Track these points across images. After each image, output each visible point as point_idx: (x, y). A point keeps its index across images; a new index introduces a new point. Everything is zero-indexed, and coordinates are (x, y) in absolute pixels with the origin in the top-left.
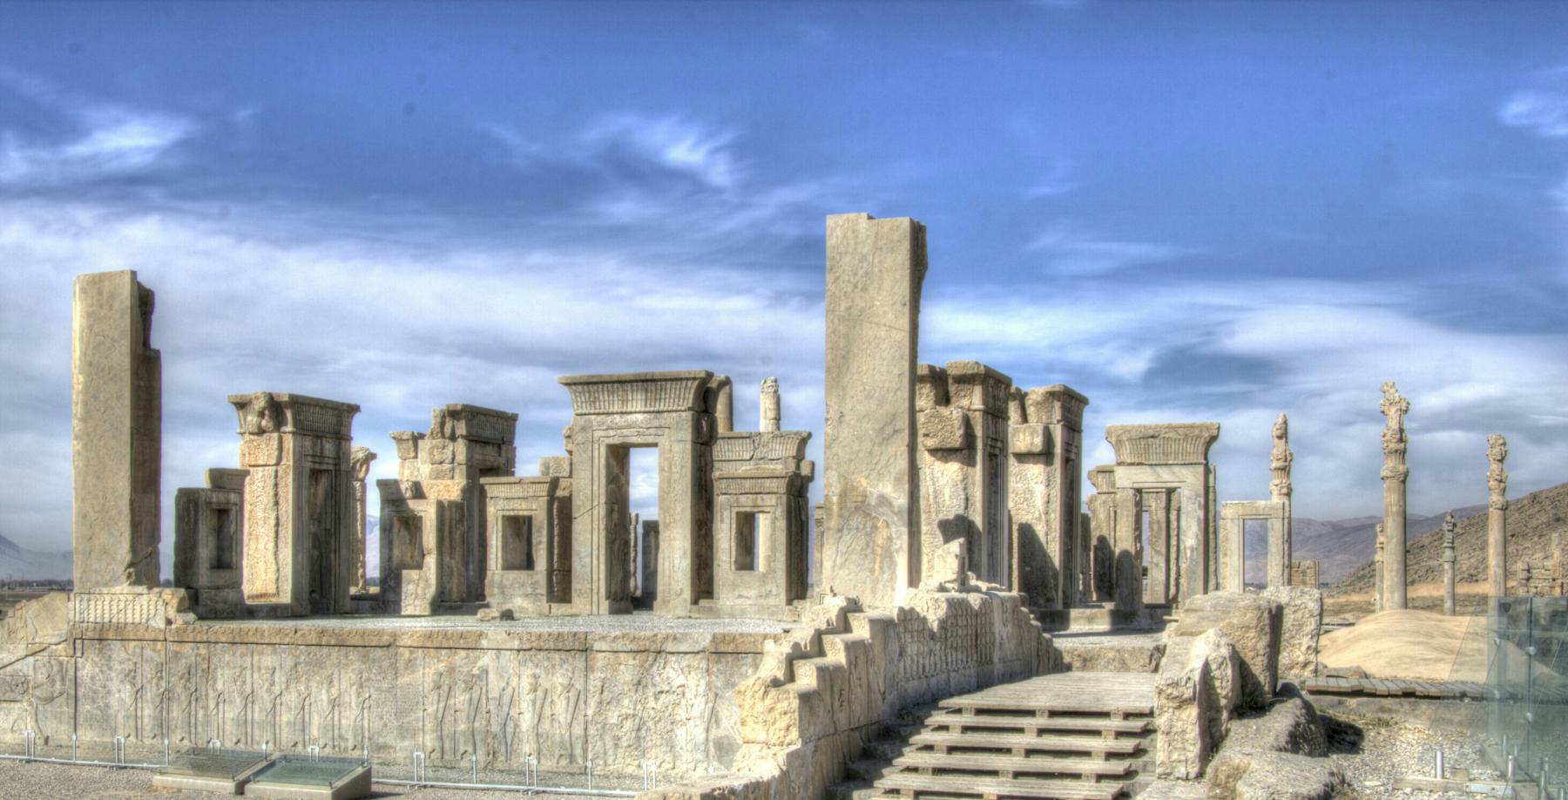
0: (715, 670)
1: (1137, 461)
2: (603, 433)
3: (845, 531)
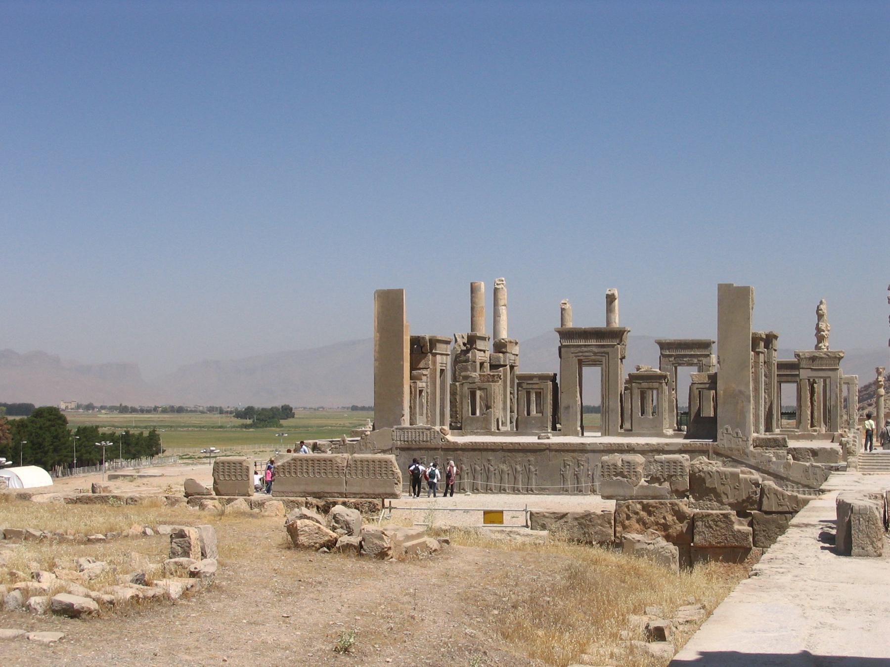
1: (808, 367)
2: (576, 355)
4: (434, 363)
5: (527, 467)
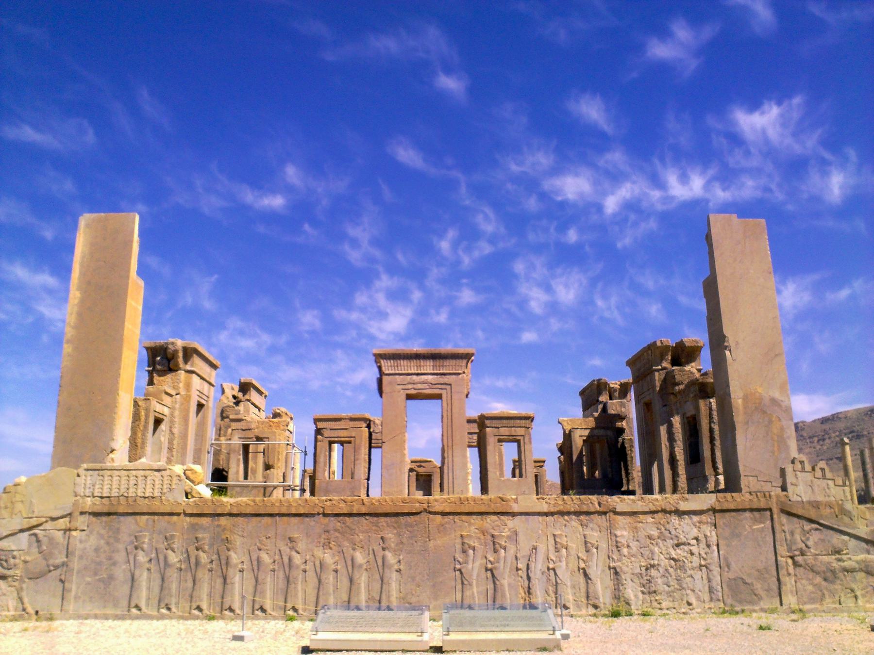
0: (721, 523)
3: (750, 423)
4: (188, 386)
5: (380, 553)
